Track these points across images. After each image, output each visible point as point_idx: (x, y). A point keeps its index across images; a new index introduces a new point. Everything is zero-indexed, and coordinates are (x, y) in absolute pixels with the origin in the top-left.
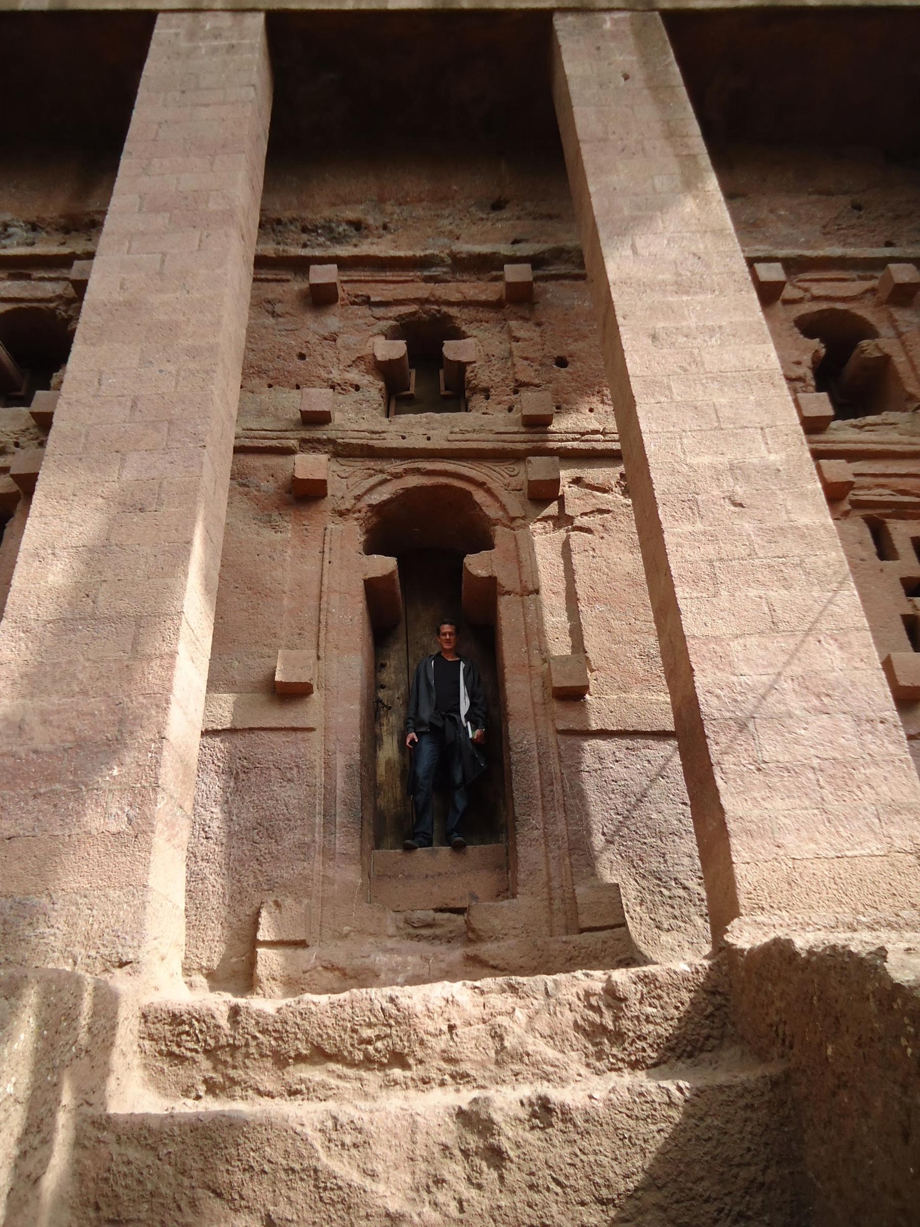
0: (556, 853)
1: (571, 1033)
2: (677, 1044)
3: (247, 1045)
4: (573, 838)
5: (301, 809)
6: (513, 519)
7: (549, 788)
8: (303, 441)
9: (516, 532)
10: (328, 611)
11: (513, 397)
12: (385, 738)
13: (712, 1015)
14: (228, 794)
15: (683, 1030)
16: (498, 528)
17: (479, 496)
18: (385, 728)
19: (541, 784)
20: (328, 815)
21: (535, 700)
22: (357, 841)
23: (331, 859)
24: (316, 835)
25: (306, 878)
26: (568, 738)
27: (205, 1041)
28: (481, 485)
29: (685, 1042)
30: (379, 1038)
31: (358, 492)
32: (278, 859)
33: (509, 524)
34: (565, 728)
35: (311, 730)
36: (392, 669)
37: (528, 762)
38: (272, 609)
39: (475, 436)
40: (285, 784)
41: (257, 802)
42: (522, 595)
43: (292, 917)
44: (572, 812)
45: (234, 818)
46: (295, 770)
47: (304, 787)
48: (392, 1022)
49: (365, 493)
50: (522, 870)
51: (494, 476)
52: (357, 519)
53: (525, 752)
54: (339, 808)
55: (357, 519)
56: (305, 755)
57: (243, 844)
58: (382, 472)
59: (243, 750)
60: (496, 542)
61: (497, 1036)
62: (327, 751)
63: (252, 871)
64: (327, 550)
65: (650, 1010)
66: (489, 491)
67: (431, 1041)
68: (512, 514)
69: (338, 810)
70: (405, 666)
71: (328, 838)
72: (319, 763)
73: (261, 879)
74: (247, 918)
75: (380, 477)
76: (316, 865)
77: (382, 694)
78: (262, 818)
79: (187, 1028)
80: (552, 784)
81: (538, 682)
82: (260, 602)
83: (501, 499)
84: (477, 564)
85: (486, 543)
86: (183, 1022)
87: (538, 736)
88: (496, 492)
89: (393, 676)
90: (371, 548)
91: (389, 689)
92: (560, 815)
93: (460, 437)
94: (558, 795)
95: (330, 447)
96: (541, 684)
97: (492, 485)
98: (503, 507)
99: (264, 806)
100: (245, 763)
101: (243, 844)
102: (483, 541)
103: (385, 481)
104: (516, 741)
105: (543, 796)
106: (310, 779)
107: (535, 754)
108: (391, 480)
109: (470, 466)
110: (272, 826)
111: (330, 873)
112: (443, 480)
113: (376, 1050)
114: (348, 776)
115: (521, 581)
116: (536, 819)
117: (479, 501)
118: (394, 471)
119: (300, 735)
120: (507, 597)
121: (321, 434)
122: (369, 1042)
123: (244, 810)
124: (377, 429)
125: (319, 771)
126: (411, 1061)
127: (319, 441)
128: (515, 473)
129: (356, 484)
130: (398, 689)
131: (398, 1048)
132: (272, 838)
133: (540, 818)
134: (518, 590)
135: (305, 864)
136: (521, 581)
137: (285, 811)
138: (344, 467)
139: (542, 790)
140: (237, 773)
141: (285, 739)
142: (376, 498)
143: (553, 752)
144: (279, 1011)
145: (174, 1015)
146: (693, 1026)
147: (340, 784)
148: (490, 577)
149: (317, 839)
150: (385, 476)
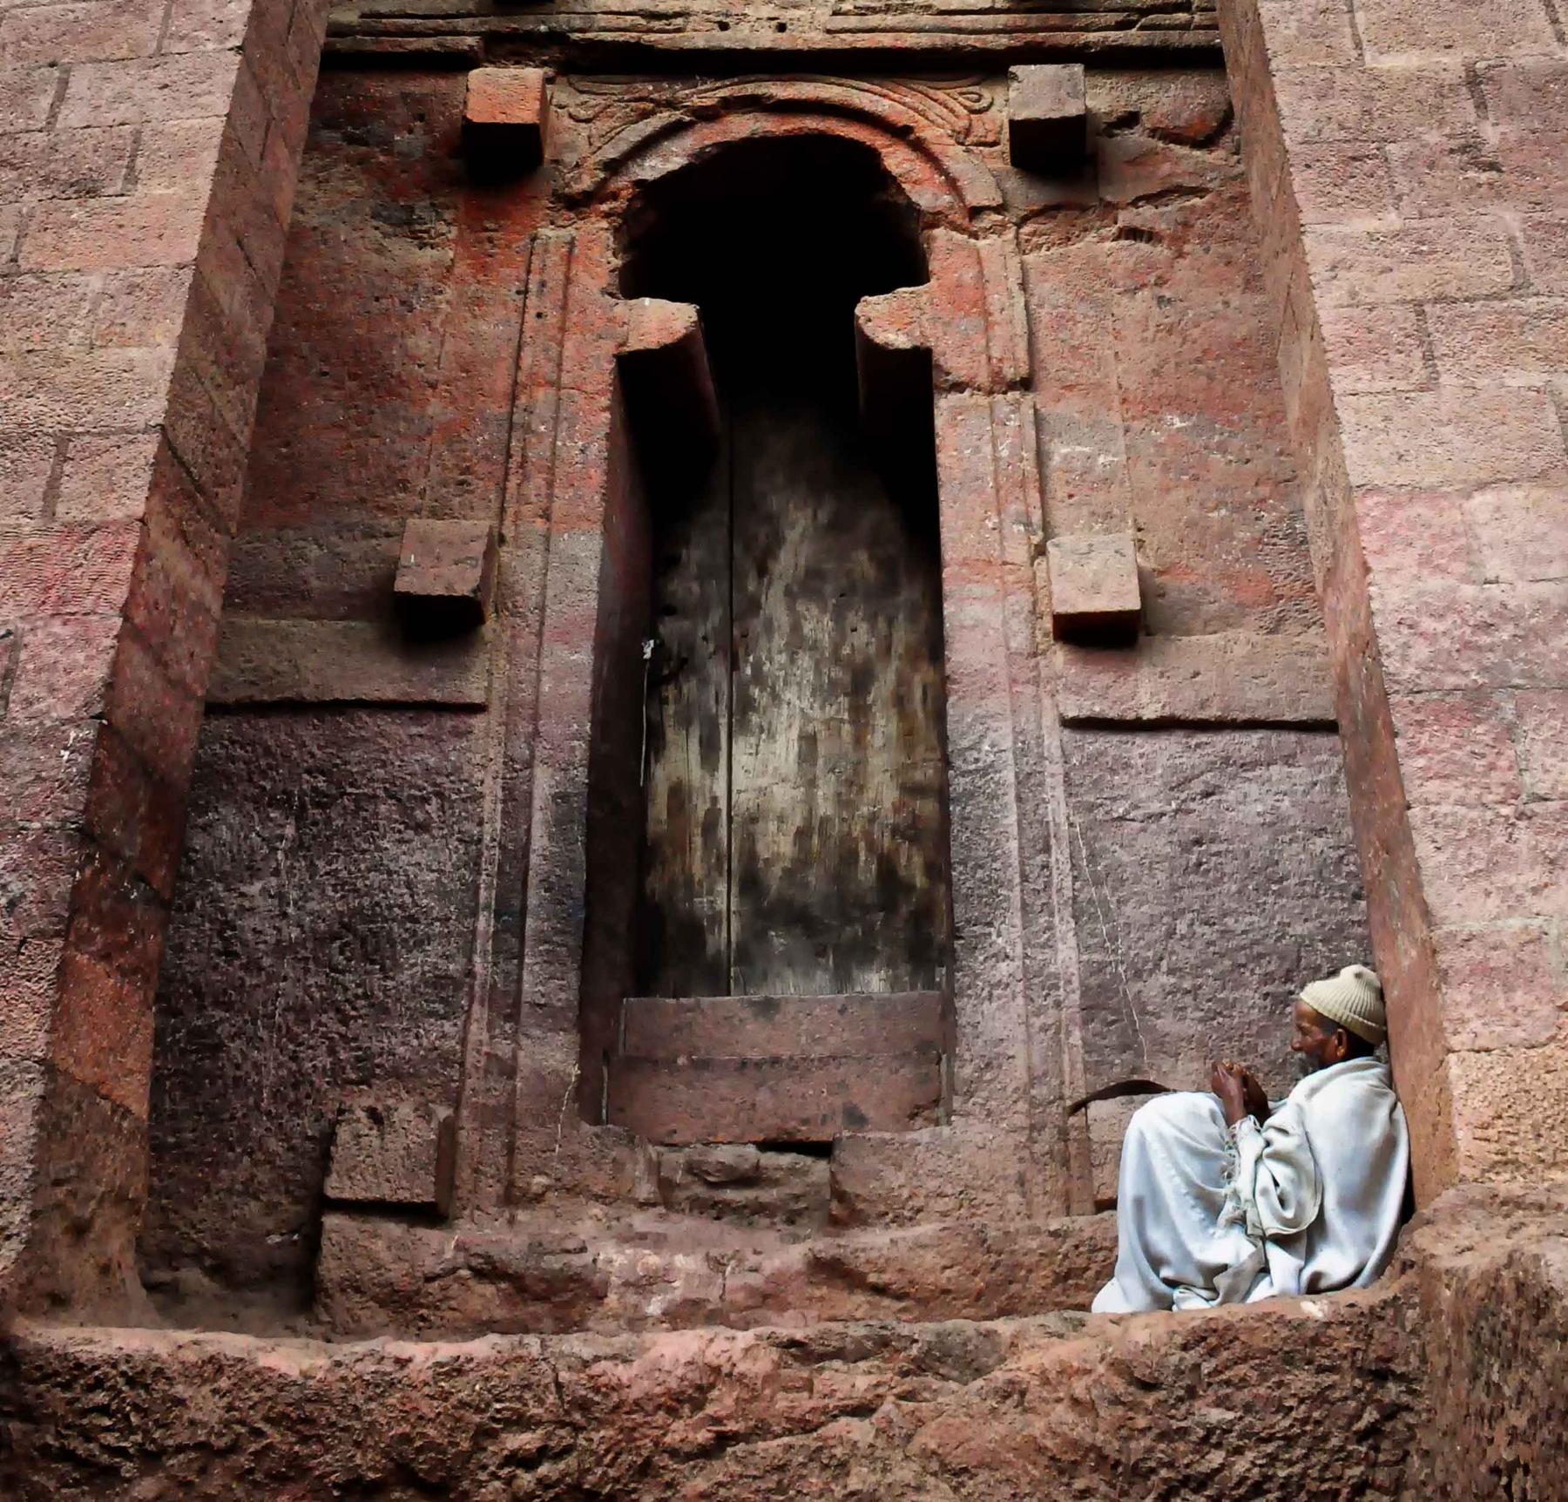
0: (1050, 1017)
4: (1093, 981)
5: (443, 895)
6: (975, 212)
7: (1041, 858)
9: (981, 243)
10: (527, 428)
12: (670, 734)
14: (280, 856)
16: (939, 232)
17: (897, 159)
18: (671, 709)
19: (1021, 848)
20: (511, 915)
21: (1013, 644)
22: (573, 979)
23: (508, 1018)
24: (477, 959)
25: (446, 1060)
26: (1090, 737)
28: (902, 134)
31: (611, 152)
32: (386, 1011)
33: (966, 222)
34: (1084, 713)
35: (478, 709)
37: (993, 797)
38: (402, 426)
39: (890, 20)
40: (409, 834)
41: (344, 874)
42: (991, 393)
43: (407, 1148)
44: (1093, 918)
45: (290, 910)
46: (434, 800)
47: (454, 843)
48: (577, 1417)
50: (967, 1056)
51: (933, 111)
52: (607, 215)
53: (984, 771)
55: (607, 215)
56: (457, 770)
57: (307, 971)
58: (671, 105)
59: (318, 753)
60: (934, 265)
62: (509, 760)
63: (324, 1035)
64: (533, 287)
65: (1216, 1415)
66: (919, 147)
68: (973, 199)
69: (532, 901)
70: (721, 560)
71: (502, 965)
72: (492, 789)
73: (343, 1056)
74: (309, 1145)
75: (664, 118)
76: (474, 1027)
78: (355, 912)
80: (1047, 849)
81: (1023, 600)
82: (374, 407)
83: (947, 163)
84: (885, 319)
85: (913, 270)
87: (1017, 733)
88: (935, 149)
90: (636, 281)
91: (686, 616)
92: (1064, 926)
93: (853, 22)
94: (1062, 876)
96: (1028, 607)
97: (928, 133)
98: (952, 184)
99: (359, 884)
100: (321, 783)
101: (307, 971)
102: (905, 266)
104: (965, 743)
105: (1025, 878)
106: (467, 826)
107: (1009, 775)
108: (690, 125)
109: (877, 89)
110: (375, 934)
111: (504, 1049)
112: (811, 123)
114: (558, 822)
115: (990, 358)
116: (1008, 934)
117: (895, 171)
118: (696, 101)
119: (449, 723)
120: (954, 398)
123: (315, 893)
125: (491, 807)
128: (984, 103)
129: (608, 137)
130: (706, 617)
132: (373, 962)
133: (1016, 933)
134: (983, 379)
135: (447, 1026)
136: (990, 358)
137: (408, 899)
139: (1022, 864)
140: (303, 807)
141: (414, 730)
142: (653, 168)
143: (1054, 769)
147: (540, 840)
148: (915, 349)
149: (478, 968)
150: (677, 115)
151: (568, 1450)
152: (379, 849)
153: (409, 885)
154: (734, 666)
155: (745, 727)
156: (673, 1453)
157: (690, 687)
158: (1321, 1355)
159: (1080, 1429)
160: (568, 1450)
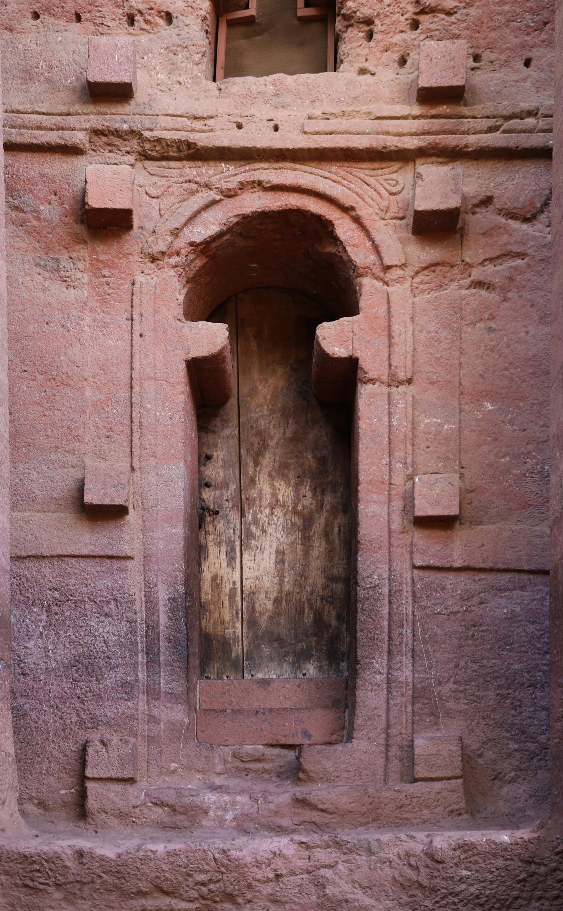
1: (388, 887)
2: (486, 901)
3: (93, 882)
8: (97, 132)
11: (410, 35)
13: (524, 880)
15: (493, 891)
27: (55, 877)
29: (494, 900)
30: (210, 881)
36: (220, 462)
49: (185, 225)
54: (163, 645)
58: (208, 186)
61: (321, 885)
67: (260, 886)
69: (162, 648)
77: (208, 495)
79: (37, 867)
86: (34, 862)
89: (221, 472)
95: (134, 144)
103: (214, 202)
113: (209, 890)
121: (118, 117)
122: (204, 884)
124: (201, 111)
126: (240, 900)
127: (117, 133)
131: (229, 890)
138: (155, 179)
144: (119, 856)
145: (25, 856)
146: (504, 888)
151: (218, 881)
152: (88, 625)
153: (105, 642)
154: (242, 515)
155: (249, 547)
156: (259, 881)
157: (220, 525)
158: (507, 855)
159: (413, 875)
160: (218, 881)
